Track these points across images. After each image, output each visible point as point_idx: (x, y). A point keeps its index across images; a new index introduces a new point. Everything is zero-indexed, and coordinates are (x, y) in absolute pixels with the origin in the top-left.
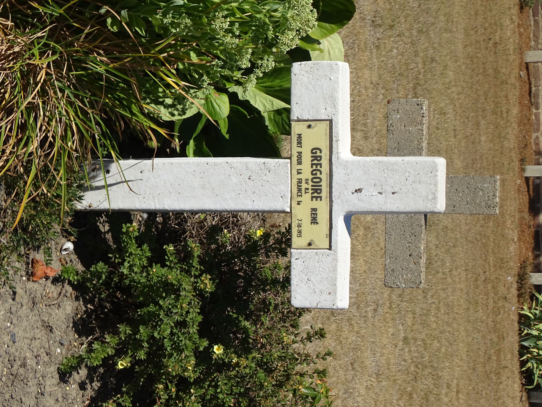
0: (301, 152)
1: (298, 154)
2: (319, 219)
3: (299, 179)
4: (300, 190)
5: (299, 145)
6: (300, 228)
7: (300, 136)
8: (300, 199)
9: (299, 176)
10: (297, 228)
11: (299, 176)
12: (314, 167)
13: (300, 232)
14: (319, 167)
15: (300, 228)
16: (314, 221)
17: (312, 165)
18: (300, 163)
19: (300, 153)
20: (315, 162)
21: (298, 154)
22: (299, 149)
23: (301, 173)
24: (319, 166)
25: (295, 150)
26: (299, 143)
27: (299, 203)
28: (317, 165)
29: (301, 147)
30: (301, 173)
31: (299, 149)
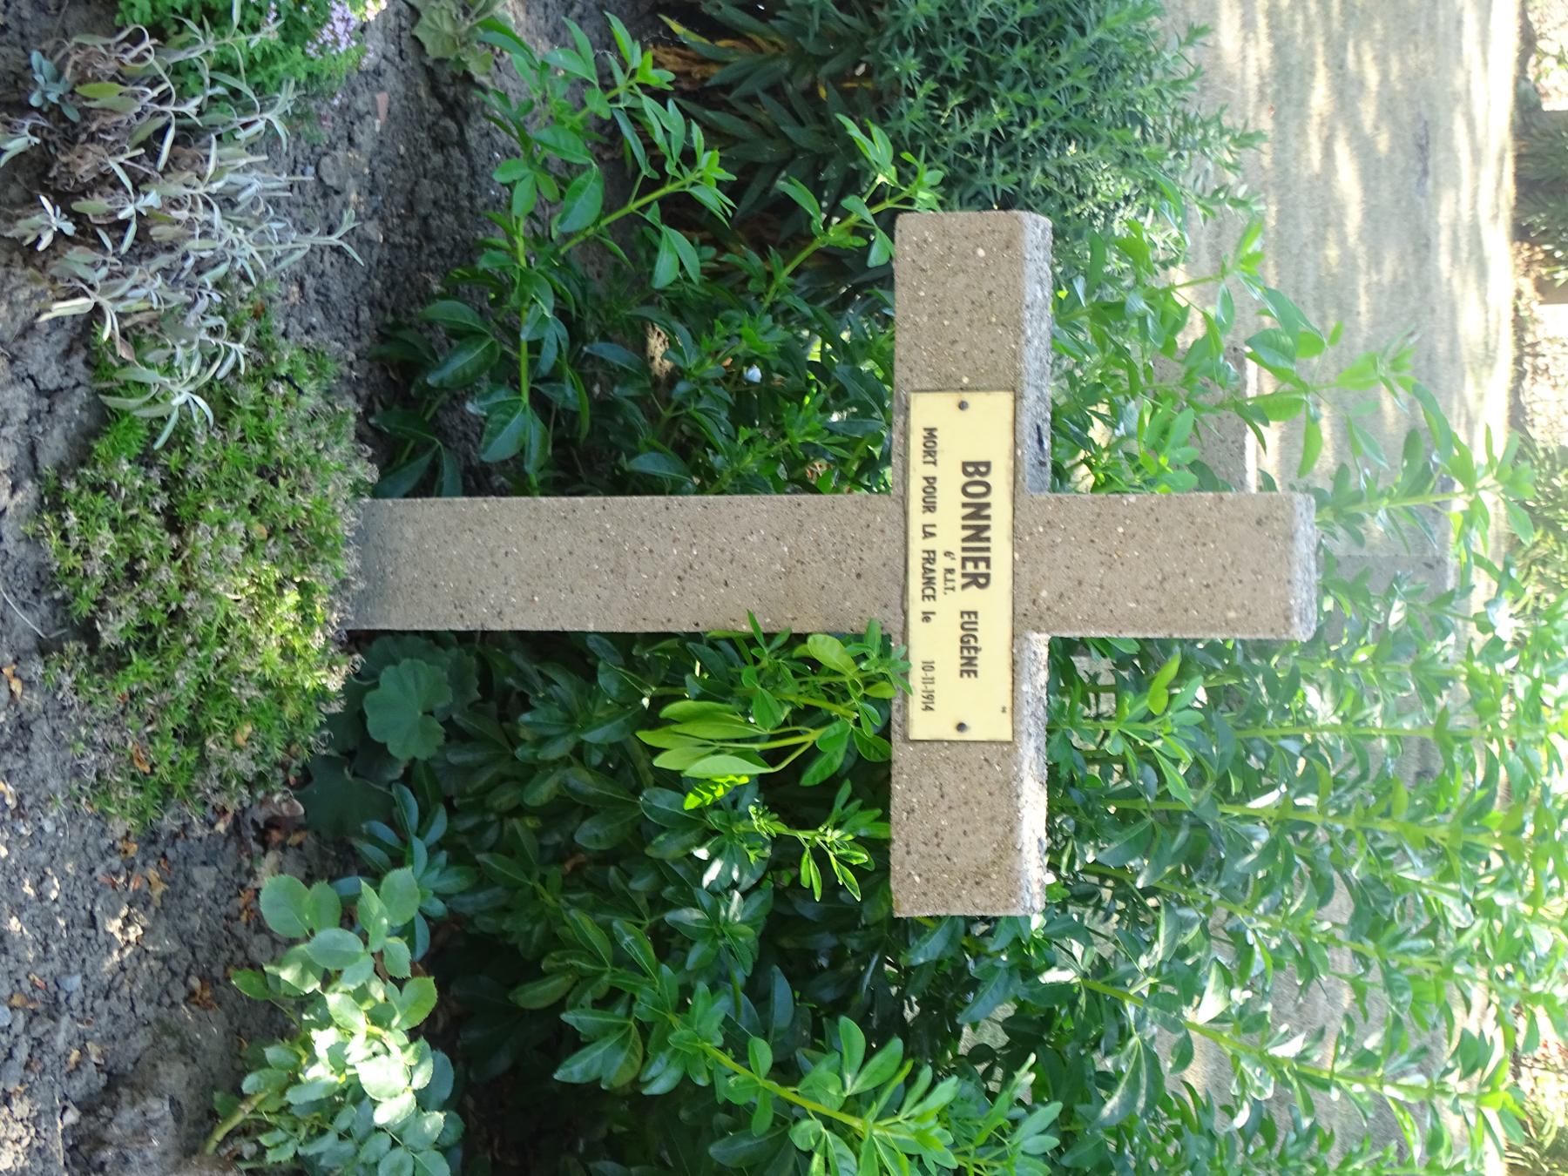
2: (982, 661)
4: (929, 582)
7: (931, 433)
8: (928, 605)
9: (930, 544)
11: (930, 544)
12: (970, 567)
14: (982, 565)
16: (969, 667)
17: (964, 560)
18: (930, 507)
19: (930, 481)
22: (930, 471)
24: (982, 565)
26: (930, 452)
27: (926, 617)
28: (976, 561)
31: (930, 471)
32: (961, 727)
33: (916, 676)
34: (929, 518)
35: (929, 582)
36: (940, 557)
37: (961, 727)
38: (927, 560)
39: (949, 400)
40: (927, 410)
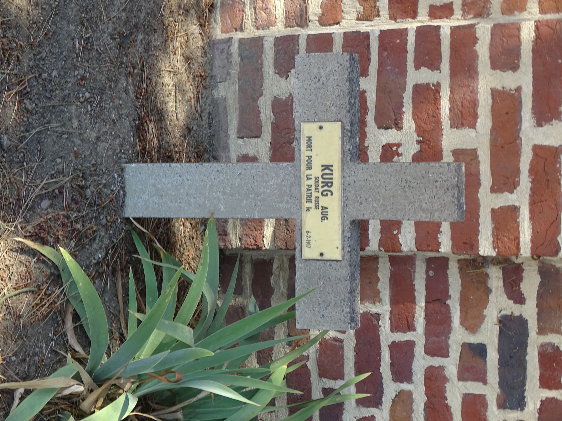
0: (311, 157)
1: (307, 158)
3: (308, 186)
5: (309, 149)
6: (309, 239)
7: (309, 138)
10: (306, 239)
13: (309, 243)
15: (309, 239)
18: (309, 168)
19: (310, 157)
20: (326, 188)
21: (307, 158)
22: (309, 153)
23: (311, 179)
25: (305, 153)
26: (309, 146)
29: (311, 150)
30: (311, 179)
31: (309, 153)
32: (322, 254)
33: (304, 234)
34: (308, 172)
35: (310, 196)
36: (313, 188)
37: (322, 254)
38: (308, 190)
39: (316, 125)
40: (308, 129)
